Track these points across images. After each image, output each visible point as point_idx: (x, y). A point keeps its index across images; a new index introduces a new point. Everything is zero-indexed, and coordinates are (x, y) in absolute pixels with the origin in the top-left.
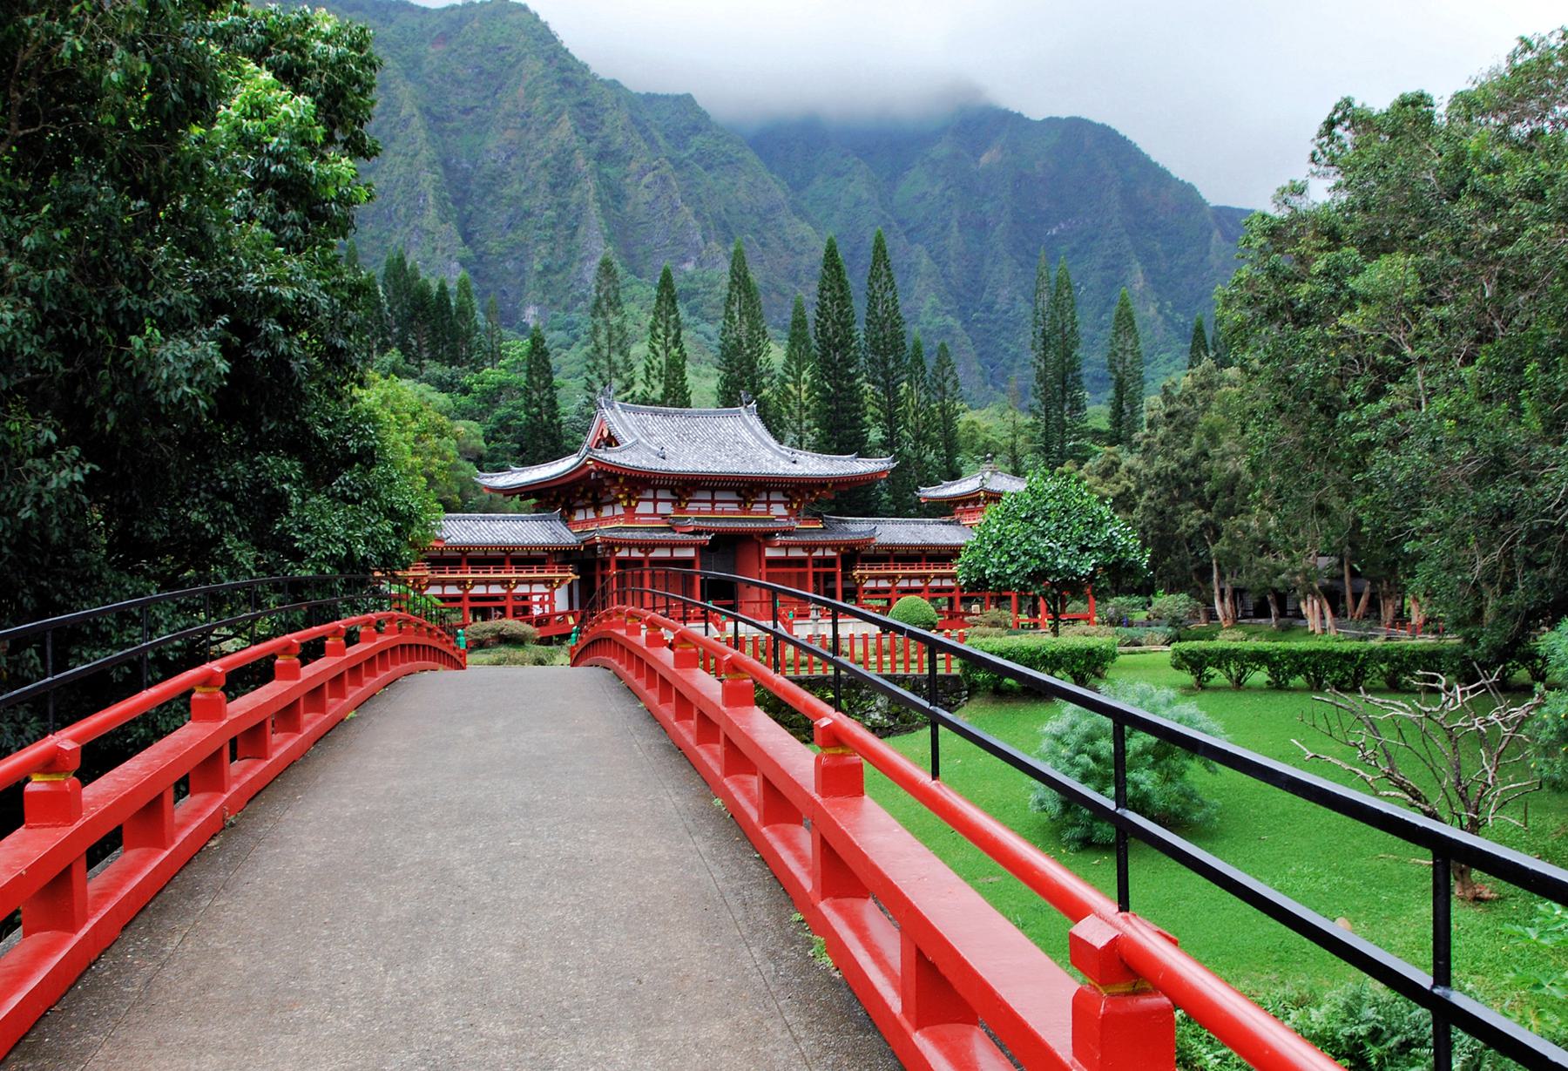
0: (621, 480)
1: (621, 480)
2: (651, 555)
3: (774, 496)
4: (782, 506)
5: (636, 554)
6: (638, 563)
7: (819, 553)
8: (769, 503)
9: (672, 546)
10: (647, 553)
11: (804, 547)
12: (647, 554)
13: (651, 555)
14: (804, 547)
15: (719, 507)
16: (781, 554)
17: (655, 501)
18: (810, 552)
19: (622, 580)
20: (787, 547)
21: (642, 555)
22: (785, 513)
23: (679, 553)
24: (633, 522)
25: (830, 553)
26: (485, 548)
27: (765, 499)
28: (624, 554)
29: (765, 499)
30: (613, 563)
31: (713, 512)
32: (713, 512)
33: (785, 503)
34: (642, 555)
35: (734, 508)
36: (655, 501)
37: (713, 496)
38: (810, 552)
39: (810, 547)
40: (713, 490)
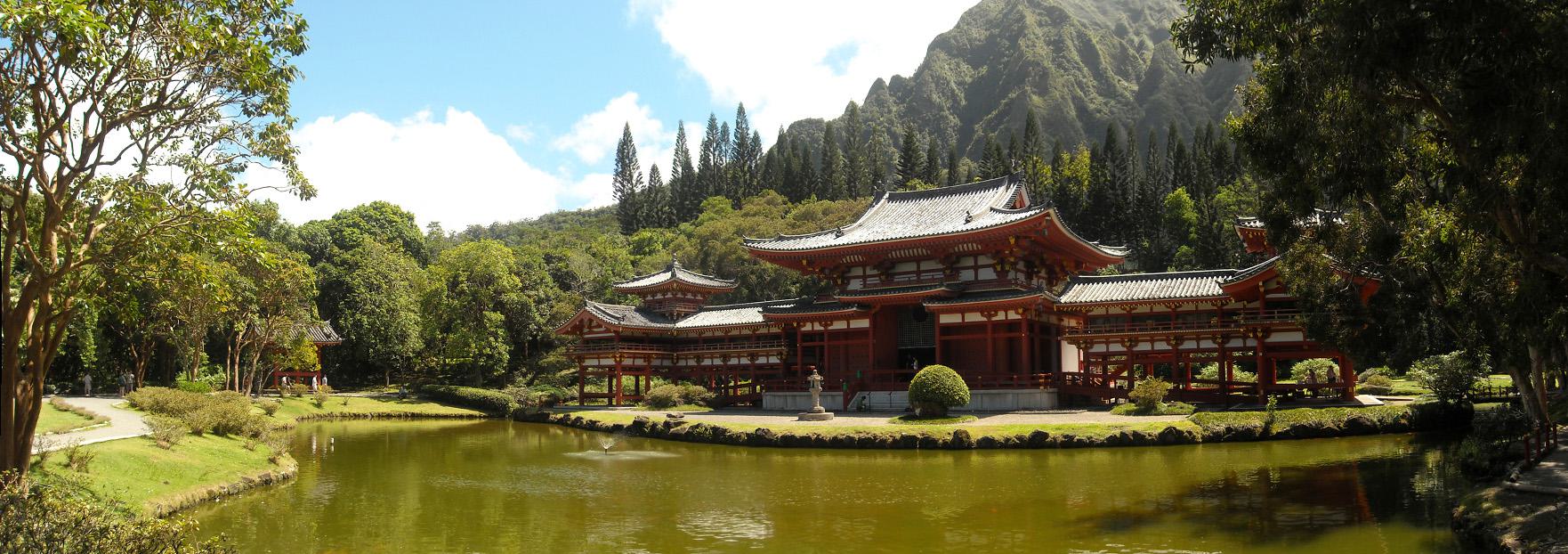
1: (804, 262)
3: (982, 260)
5: (818, 327)
6: (821, 334)
7: (1001, 316)
8: (976, 268)
9: (848, 318)
10: (826, 326)
12: (826, 326)
13: (830, 328)
16: (955, 319)
18: (990, 316)
20: (962, 311)
21: (822, 328)
22: (994, 276)
24: (823, 300)
25: (1012, 315)
27: (973, 264)
28: (808, 327)
29: (973, 264)
30: (799, 337)
32: (919, 281)
33: (993, 266)
34: (822, 328)
35: (939, 275)
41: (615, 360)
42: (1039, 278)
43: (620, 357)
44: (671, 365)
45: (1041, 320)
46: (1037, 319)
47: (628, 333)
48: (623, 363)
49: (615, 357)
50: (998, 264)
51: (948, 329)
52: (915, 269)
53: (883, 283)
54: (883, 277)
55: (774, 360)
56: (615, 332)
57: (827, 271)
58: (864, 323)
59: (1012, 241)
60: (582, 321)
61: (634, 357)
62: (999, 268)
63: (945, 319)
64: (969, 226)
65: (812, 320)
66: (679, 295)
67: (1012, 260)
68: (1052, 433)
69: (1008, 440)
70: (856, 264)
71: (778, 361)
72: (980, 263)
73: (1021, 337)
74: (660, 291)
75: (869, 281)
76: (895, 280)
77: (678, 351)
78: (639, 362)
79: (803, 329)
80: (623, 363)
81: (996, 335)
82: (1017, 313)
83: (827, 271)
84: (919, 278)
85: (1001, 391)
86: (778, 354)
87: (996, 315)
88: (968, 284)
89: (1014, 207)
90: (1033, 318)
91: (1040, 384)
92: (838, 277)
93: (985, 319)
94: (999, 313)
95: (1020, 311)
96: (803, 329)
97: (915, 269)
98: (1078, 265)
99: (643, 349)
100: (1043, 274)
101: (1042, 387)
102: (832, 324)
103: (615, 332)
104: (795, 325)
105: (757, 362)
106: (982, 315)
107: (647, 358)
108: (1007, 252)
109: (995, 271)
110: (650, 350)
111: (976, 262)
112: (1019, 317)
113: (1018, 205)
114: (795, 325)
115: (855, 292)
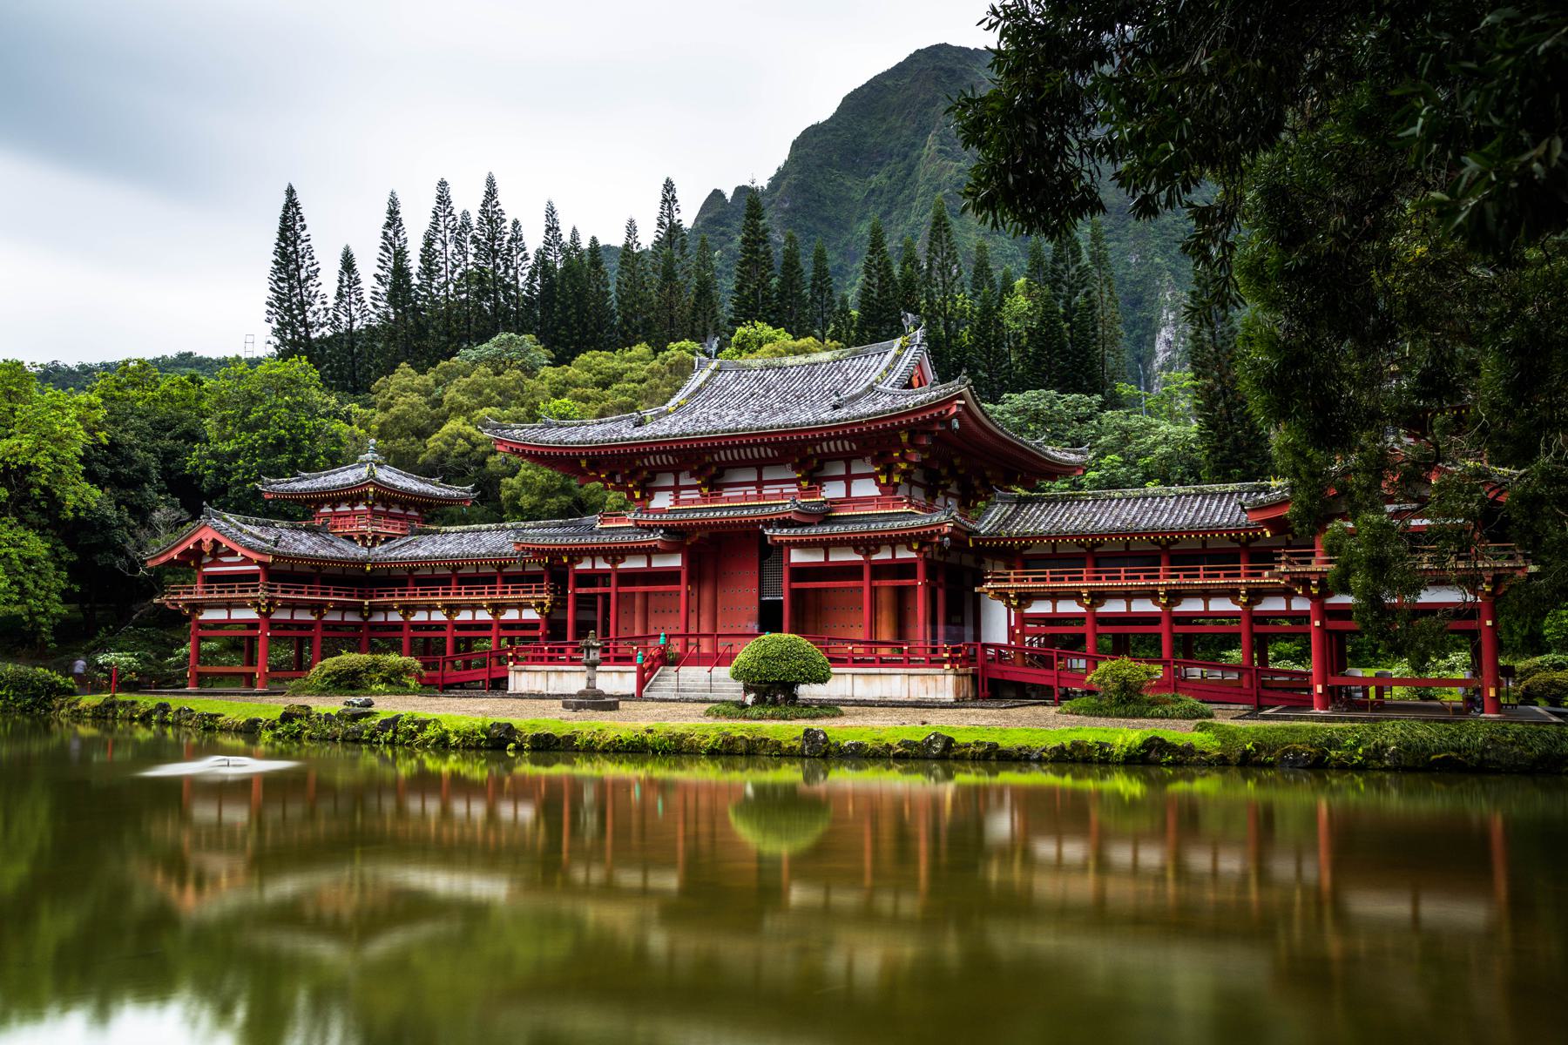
0: (584, 463)
1: (584, 463)
2: (620, 566)
4: (872, 481)
5: (602, 565)
7: (884, 555)
8: (848, 479)
9: (649, 552)
10: (614, 562)
11: (855, 544)
12: (614, 562)
13: (620, 566)
14: (855, 544)
15: (768, 490)
16: (817, 558)
17: (677, 489)
18: (868, 553)
19: (585, 602)
20: (826, 545)
21: (608, 566)
22: (875, 491)
23: (658, 563)
24: (611, 522)
25: (903, 554)
26: (478, 561)
27: (844, 473)
28: (585, 565)
29: (844, 473)
31: (760, 496)
32: (760, 496)
33: (875, 476)
34: (608, 566)
36: (677, 489)
37: (760, 476)
38: (868, 553)
39: (867, 544)
40: (759, 465)
41: (259, 612)
42: (947, 495)
43: (269, 605)
44: (360, 620)
45: (948, 560)
46: (942, 559)
47: (284, 566)
48: (273, 617)
49: (256, 605)
50: (882, 472)
51: (800, 572)
52: (755, 478)
53: (704, 498)
54: (705, 491)
55: (531, 615)
56: (259, 563)
57: (618, 479)
58: (676, 562)
59: (904, 438)
60: (199, 543)
61: (293, 606)
62: (883, 480)
63: (797, 557)
64: (842, 413)
65: (593, 553)
66: (379, 508)
67: (903, 466)
68: (961, 739)
69: (889, 747)
70: (665, 469)
71: (537, 617)
72: (854, 472)
73: (915, 587)
74: (344, 499)
75: (684, 495)
76: (724, 495)
77: (371, 597)
78: (303, 616)
79: (578, 567)
80: (273, 617)
81: (876, 583)
82: (910, 549)
83: (618, 479)
84: (760, 492)
85: (883, 670)
86: (537, 606)
87: (877, 551)
88: (832, 501)
89: (909, 386)
90: (936, 557)
91: (944, 661)
92: (636, 488)
93: (860, 558)
94: (883, 548)
95: (916, 547)
96: (578, 567)
97: (755, 478)
98: (1009, 479)
99: (310, 594)
100: (953, 489)
101: (947, 666)
102: (623, 561)
103: (259, 563)
104: (565, 560)
105: (502, 618)
106: (857, 552)
107: (317, 607)
108: (896, 455)
109: (878, 483)
110: (323, 594)
111: (848, 469)
112: (913, 555)
113: (915, 381)
114: (565, 560)
115: (661, 511)
